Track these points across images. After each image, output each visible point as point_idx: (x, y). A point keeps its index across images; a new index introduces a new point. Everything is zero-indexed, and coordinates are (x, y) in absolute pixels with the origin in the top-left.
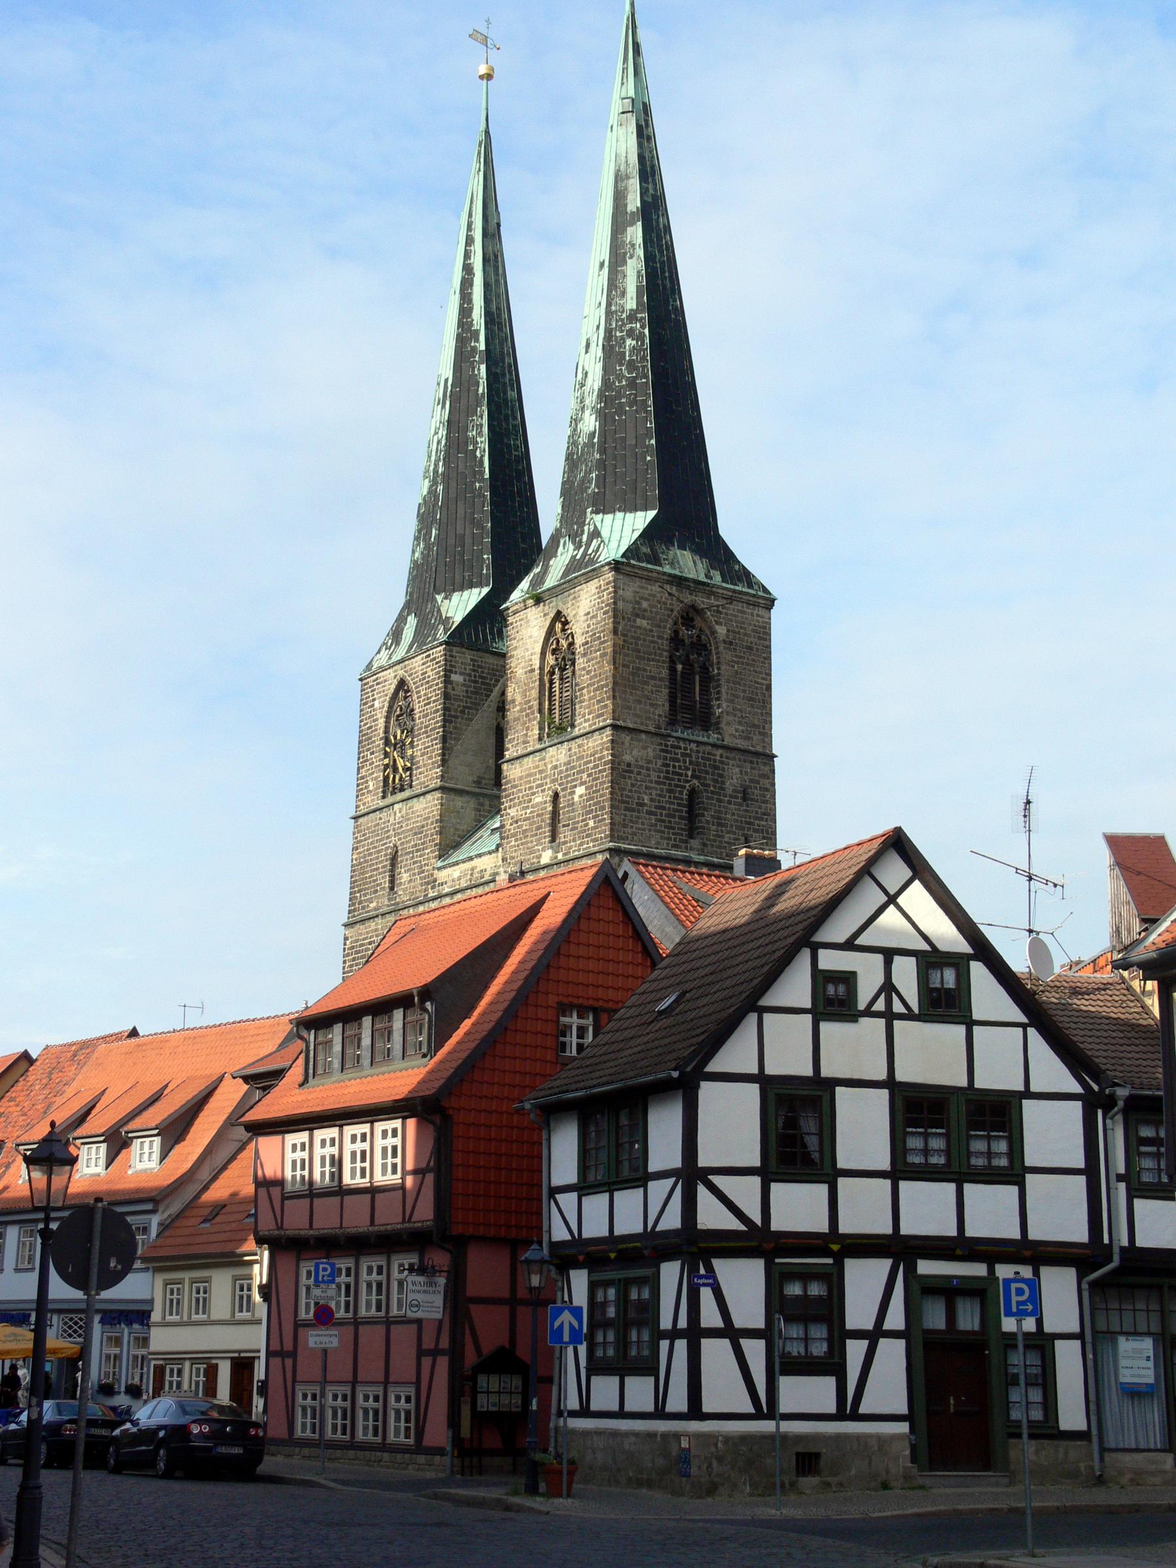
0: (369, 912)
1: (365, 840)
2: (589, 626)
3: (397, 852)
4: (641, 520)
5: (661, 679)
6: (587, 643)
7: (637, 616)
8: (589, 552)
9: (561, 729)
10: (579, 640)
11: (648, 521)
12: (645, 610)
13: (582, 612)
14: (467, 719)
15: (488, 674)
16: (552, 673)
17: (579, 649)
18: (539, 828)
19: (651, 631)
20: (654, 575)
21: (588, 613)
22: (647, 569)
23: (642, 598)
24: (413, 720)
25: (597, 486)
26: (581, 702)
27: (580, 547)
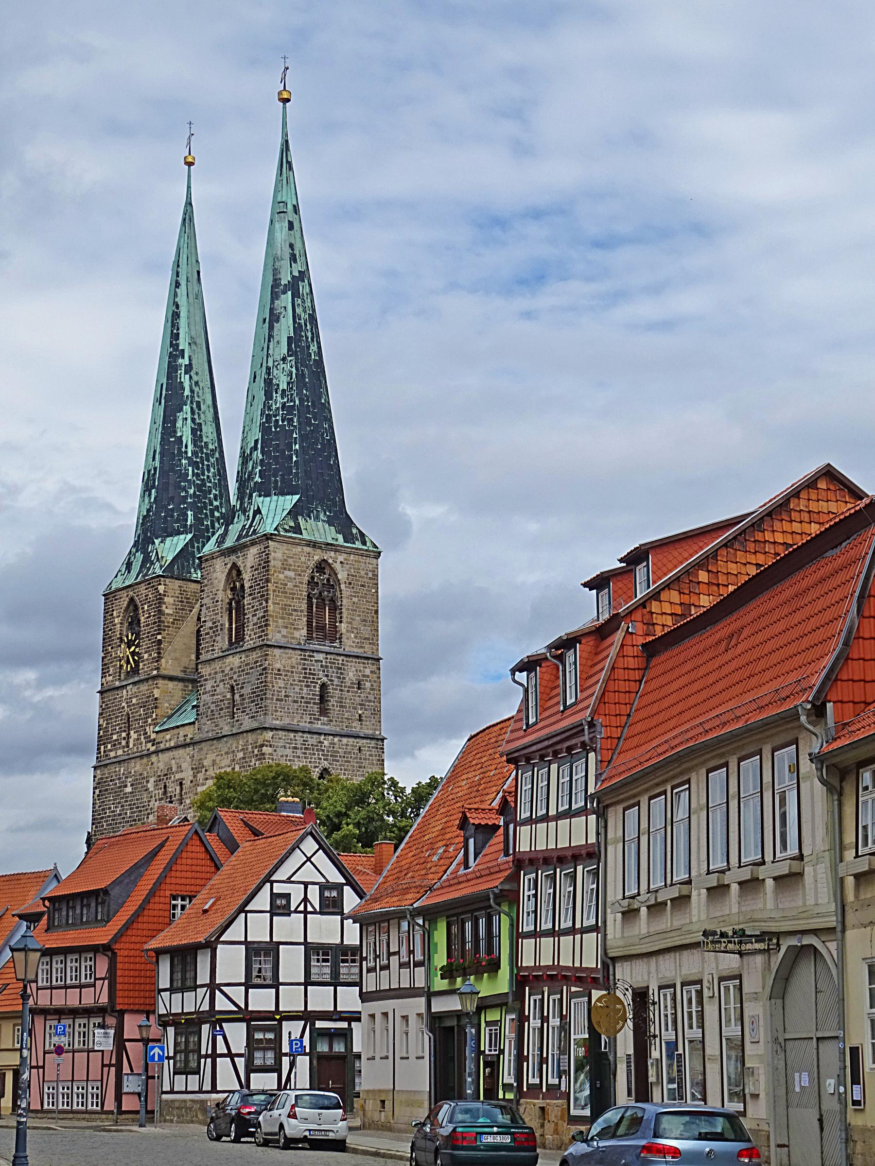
0: (110, 759)
1: (108, 708)
2: (253, 576)
3: (129, 718)
4: (290, 501)
6: (251, 587)
7: (285, 569)
8: (254, 525)
9: (237, 642)
10: (247, 585)
11: (293, 503)
12: (291, 565)
13: (249, 565)
14: (176, 628)
15: (191, 595)
16: (230, 604)
17: (247, 591)
18: (221, 709)
20: (297, 541)
21: (253, 567)
22: (291, 537)
23: (288, 557)
24: (140, 627)
25: (260, 477)
26: (247, 626)
27: (248, 519)
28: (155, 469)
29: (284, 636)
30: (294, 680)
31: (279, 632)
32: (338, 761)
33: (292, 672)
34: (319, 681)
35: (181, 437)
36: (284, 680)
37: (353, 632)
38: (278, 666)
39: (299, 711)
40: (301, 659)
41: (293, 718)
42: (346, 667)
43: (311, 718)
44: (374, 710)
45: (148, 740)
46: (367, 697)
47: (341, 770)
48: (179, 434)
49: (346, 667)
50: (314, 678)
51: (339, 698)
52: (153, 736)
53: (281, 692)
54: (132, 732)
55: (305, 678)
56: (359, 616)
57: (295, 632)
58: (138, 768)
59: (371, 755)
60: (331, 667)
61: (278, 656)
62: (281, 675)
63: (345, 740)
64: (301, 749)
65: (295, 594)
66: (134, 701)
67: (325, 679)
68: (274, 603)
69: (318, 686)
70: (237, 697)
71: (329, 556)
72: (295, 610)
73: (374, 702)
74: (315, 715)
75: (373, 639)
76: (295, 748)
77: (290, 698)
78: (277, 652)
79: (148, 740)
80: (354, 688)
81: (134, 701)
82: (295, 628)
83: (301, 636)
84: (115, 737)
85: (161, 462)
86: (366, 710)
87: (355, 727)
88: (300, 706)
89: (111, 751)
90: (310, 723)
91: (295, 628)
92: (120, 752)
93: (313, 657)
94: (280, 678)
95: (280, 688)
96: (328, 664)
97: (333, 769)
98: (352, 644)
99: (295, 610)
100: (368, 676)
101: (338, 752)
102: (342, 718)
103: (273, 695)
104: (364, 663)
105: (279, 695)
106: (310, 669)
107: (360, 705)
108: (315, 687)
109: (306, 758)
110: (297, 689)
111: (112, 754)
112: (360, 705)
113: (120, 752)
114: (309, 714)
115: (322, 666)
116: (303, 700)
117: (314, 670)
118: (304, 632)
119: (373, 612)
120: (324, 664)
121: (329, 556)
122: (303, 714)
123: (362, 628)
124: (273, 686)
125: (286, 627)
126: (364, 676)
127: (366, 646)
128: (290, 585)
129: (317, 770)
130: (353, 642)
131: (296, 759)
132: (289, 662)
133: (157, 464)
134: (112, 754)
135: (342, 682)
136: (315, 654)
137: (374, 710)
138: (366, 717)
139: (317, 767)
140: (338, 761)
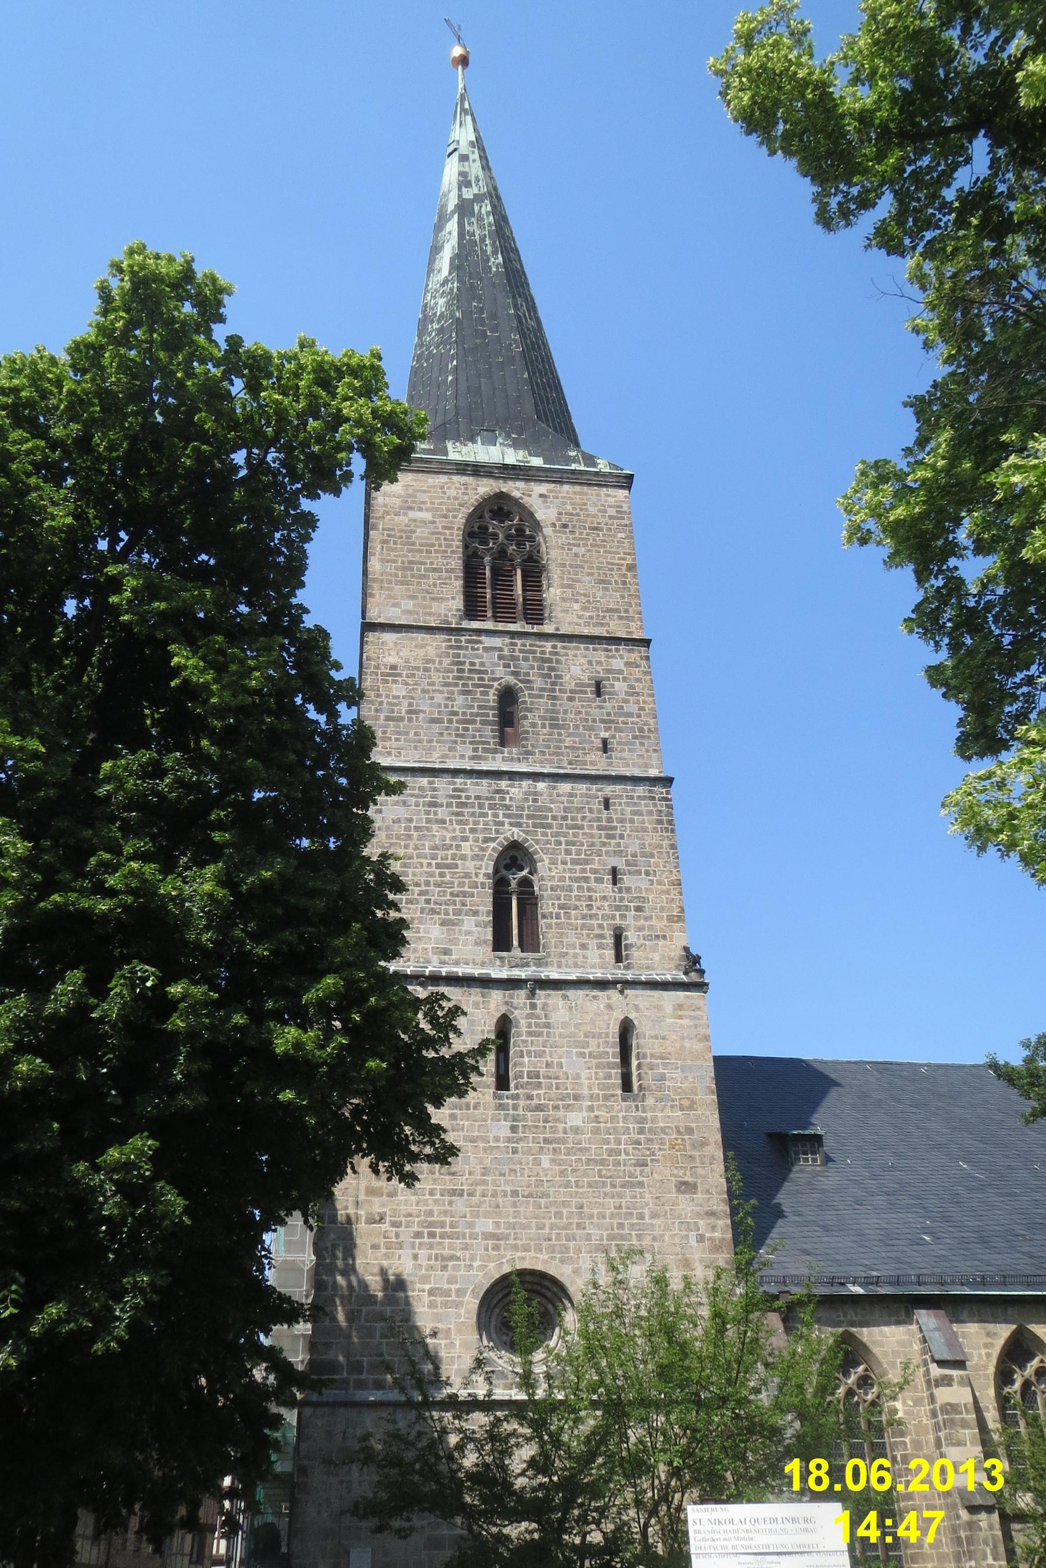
5: (452, 570)
7: (411, 508)
19: (434, 522)
29: (408, 612)
30: (433, 684)
31: (396, 605)
32: (550, 826)
33: (426, 670)
34: (496, 684)
36: (407, 684)
37: (577, 601)
38: (392, 660)
39: (445, 738)
40: (451, 647)
41: (429, 751)
42: (563, 659)
43: (475, 750)
44: (641, 730)
46: (622, 708)
47: (560, 843)
49: (563, 659)
50: (482, 679)
51: (547, 711)
53: (399, 704)
55: (460, 678)
56: (589, 574)
57: (434, 604)
59: (639, 813)
60: (526, 659)
61: (391, 645)
62: (399, 675)
63: (565, 787)
64: (449, 805)
65: (434, 545)
67: (511, 680)
68: (383, 561)
69: (492, 691)
71: (515, 489)
73: (639, 716)
74: (488, 743)
75: (626, 611)
76: (433, 804)
77: (421, 715)
78: (389, 637)
80: (585, 692)
82: (433, 599)
83: (450, 610)
86: (617, 729)
87: (592, 763)
88: (447, 728)
90: (473, 758)
91: (433, 599)
93: (480, 642)
94: (395, 682)
95: (397, 697)
96: (517, 654)
97: (537, 842)
98: (576, 620)
100: (620, 672)
101: (550, 810)
102: (559, 748)
103: (377, 710)
104: (607, 650)
105: (393, 711)
106: (472, 664)
107: (603, 721)
108: (486, 693)
109: (459, 822)
110: (439, 698)
112: (603, 721)
114: (471, 743)
115: (500, 658)
116: (455, 718)
117: (482, 664)
118: (458, 603)
119: (624, 568)
120: (506, 653)
121: (515, 489)
122: (456, 742)
123: (600, 594)
124: (378, 696)
126: (608, 671)
127: (611, 623)
129: (492, 845)
130: (579, 617)
131: (435, 827)
132: (421, 652)
135: (554, 684)
136: (483, 638)
137: (641, 730)
138: (619, 743)
139: (494, 840)
140: (550, 826)
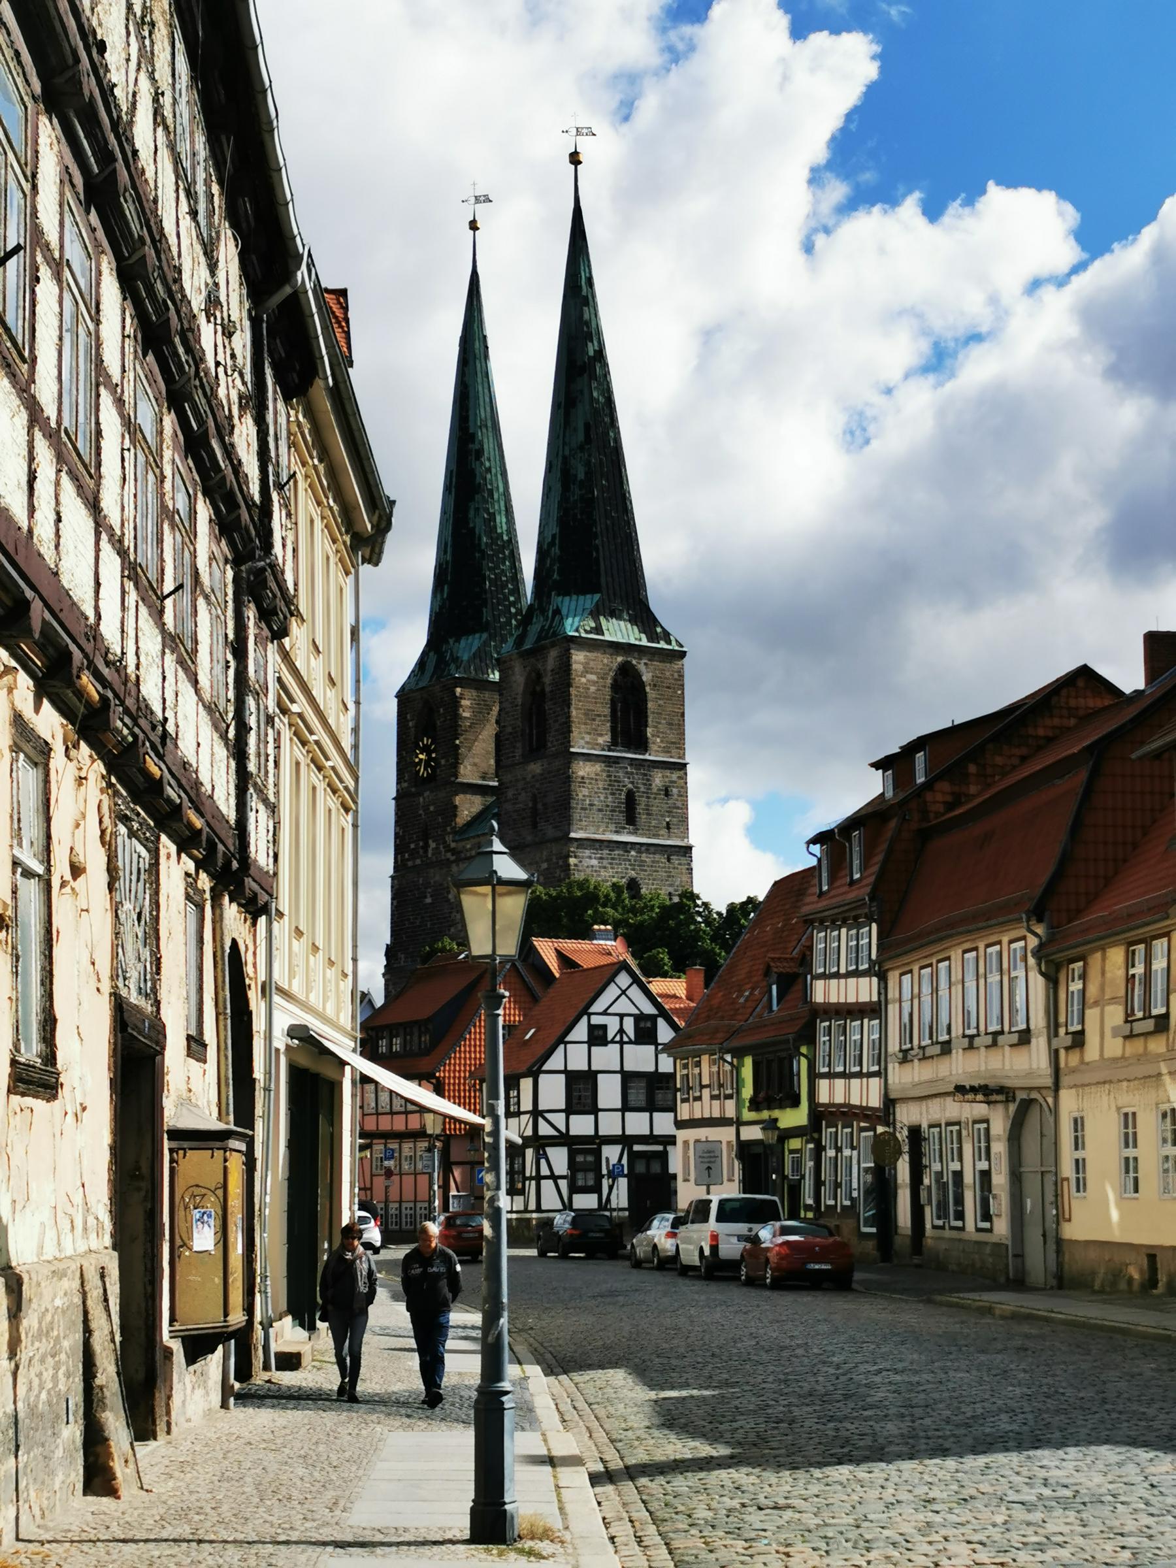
28: (447, 562)
31: (583, 738)
35: (474, 528)
45: (449, 849)
48: (471, 525)
52: (453, 845)
54: (430, 842)
58: (437, 878)
66: (432, 808)
70: (540, 806)
72: (599, 716)
79: (449, 849)
81: (432, 808)
84: (412, 846)
85: (453, 555)
89: (408, 860)
92: (418, 862)
99: (599, 716)
111: (410, 864)
113: (418, 862)
125: (589, 733)
128: (593, 689)
133: (449, 557)
134: (410, 864)
